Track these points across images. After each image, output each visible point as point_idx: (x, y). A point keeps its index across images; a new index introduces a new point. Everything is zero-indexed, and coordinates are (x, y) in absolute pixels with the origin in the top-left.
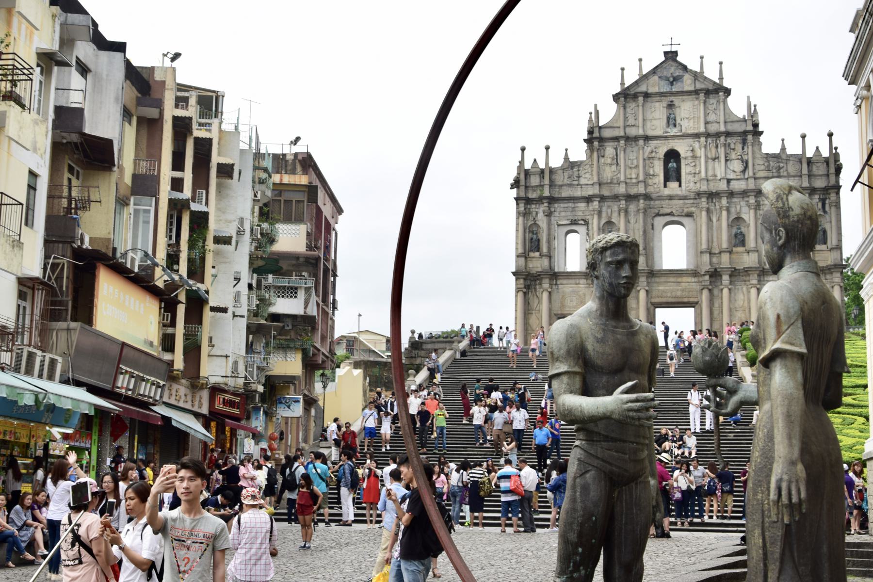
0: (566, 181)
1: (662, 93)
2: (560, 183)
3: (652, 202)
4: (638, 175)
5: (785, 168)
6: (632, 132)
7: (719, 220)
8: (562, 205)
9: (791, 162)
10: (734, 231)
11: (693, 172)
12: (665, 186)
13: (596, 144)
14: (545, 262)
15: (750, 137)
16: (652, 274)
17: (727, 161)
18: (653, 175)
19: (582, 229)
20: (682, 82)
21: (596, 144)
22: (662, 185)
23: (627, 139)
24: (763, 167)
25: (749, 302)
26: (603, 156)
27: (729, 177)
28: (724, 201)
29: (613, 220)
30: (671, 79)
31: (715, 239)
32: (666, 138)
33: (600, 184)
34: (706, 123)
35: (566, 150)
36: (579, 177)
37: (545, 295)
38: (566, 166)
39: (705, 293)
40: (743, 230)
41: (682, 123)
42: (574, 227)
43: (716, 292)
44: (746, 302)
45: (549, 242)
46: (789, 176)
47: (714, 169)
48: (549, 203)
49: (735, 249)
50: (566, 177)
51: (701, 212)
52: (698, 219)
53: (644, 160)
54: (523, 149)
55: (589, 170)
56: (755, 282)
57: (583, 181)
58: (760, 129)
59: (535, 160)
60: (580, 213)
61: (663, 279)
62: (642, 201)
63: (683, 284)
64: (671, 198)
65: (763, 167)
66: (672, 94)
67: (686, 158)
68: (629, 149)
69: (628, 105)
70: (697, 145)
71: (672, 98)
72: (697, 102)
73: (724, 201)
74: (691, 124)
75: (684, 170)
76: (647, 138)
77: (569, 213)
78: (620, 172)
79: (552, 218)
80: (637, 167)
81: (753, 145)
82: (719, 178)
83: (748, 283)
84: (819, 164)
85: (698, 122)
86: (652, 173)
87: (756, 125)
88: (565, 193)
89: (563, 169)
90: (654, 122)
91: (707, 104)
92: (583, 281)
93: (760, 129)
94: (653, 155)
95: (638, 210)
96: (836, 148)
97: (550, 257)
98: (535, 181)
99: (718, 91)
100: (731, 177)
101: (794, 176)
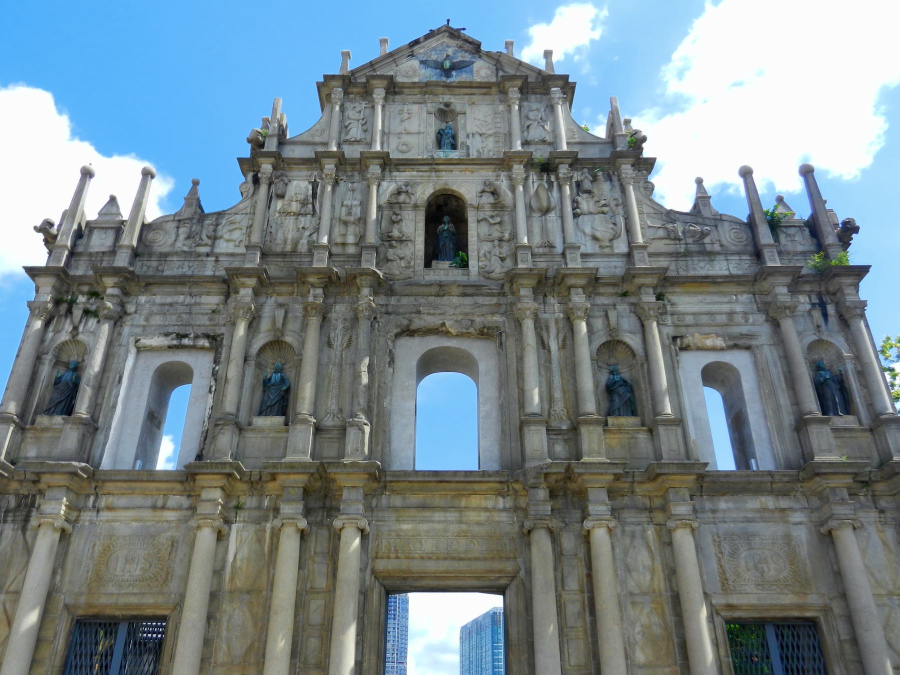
0: (181, 245)
1: (427, 84)
2: (165, 250)
3: (393, 300)
4: (362, 237)
5: (714, 236)
6: (352, 152)
7: (563, 346)
8: (158, 299)
9: (726, 224)
10: (604, 377)
11: (496, 234)
12: (428, 265)
13: (266, 167)
14: (71, 439)
15: (627, 169)
16: (381, 479)
17: (576, 216)
18: (400, 241)
19: (201, 364)
20: (472, 72)
21: (266, 167)
22: (422, 263)
23: (341, 161)
24: (661, 233)
25: (672, 572)
26: (281, 196)
27: (583, 249)
28: (578, 299)
29: (288, 339)
30: (447, 64)
31: (558, 394)
32: (431, 164)
33: (264, 255)
34: (525, 143)
35: (196, 183)
36: (214, 238)
37: (44, 544)
38: (187, 214)
39: (542, 544)
40: (625, 374)
41: (469, 142)
42: (182, 357)
43: (569, 542)
44: (660, 575)
45: (99, 388)
46: (726, 253)
47: (544, 230)
48: (126, 293)
49: (610, 420)
50: (182, 237)
51: (518, 324)
52: (510, 343)
53: (379, 207)
54: (87, 174)
55: (245, 223)
56: (682, 509)
57: (223, 247)
58: (647, 153)
59: (113, 200)
60: (204, 320)
61: (415, 499)
62: (366, 291)
63: (472, 516)
64: (442, 289)
65: (661, 233)
66: (448, 86)
67: (478, 208)
68: (342, 186)
69: (348, 105)
70: (503, 185)
71: (447, 98)
72: (501, 108)
73: (578, 299)
74: (490, 143)
75: (474, 231)
76: (387, 163)
77: (172, 319)
78: (317, 230)
79: (126, 330)
80: (363, 220)
81: (636, 182)
82: (559, 249)
83: (659, 517)
84: (792, 231)
85: (509, 136)
86: (396, 233)
87: (637, 141)
88: (173, 269)
89: (179, 220)
90: (407, 139)
91: (524, 111)
92: (175, 500)
93: (647, 153)
94: (402, 198)
95: (355, 319)
96: (826, 202)
97: (97, 429)
98: (99, 242)
99: (546, 86)
100: (589, 250)
101: (739, 253)
